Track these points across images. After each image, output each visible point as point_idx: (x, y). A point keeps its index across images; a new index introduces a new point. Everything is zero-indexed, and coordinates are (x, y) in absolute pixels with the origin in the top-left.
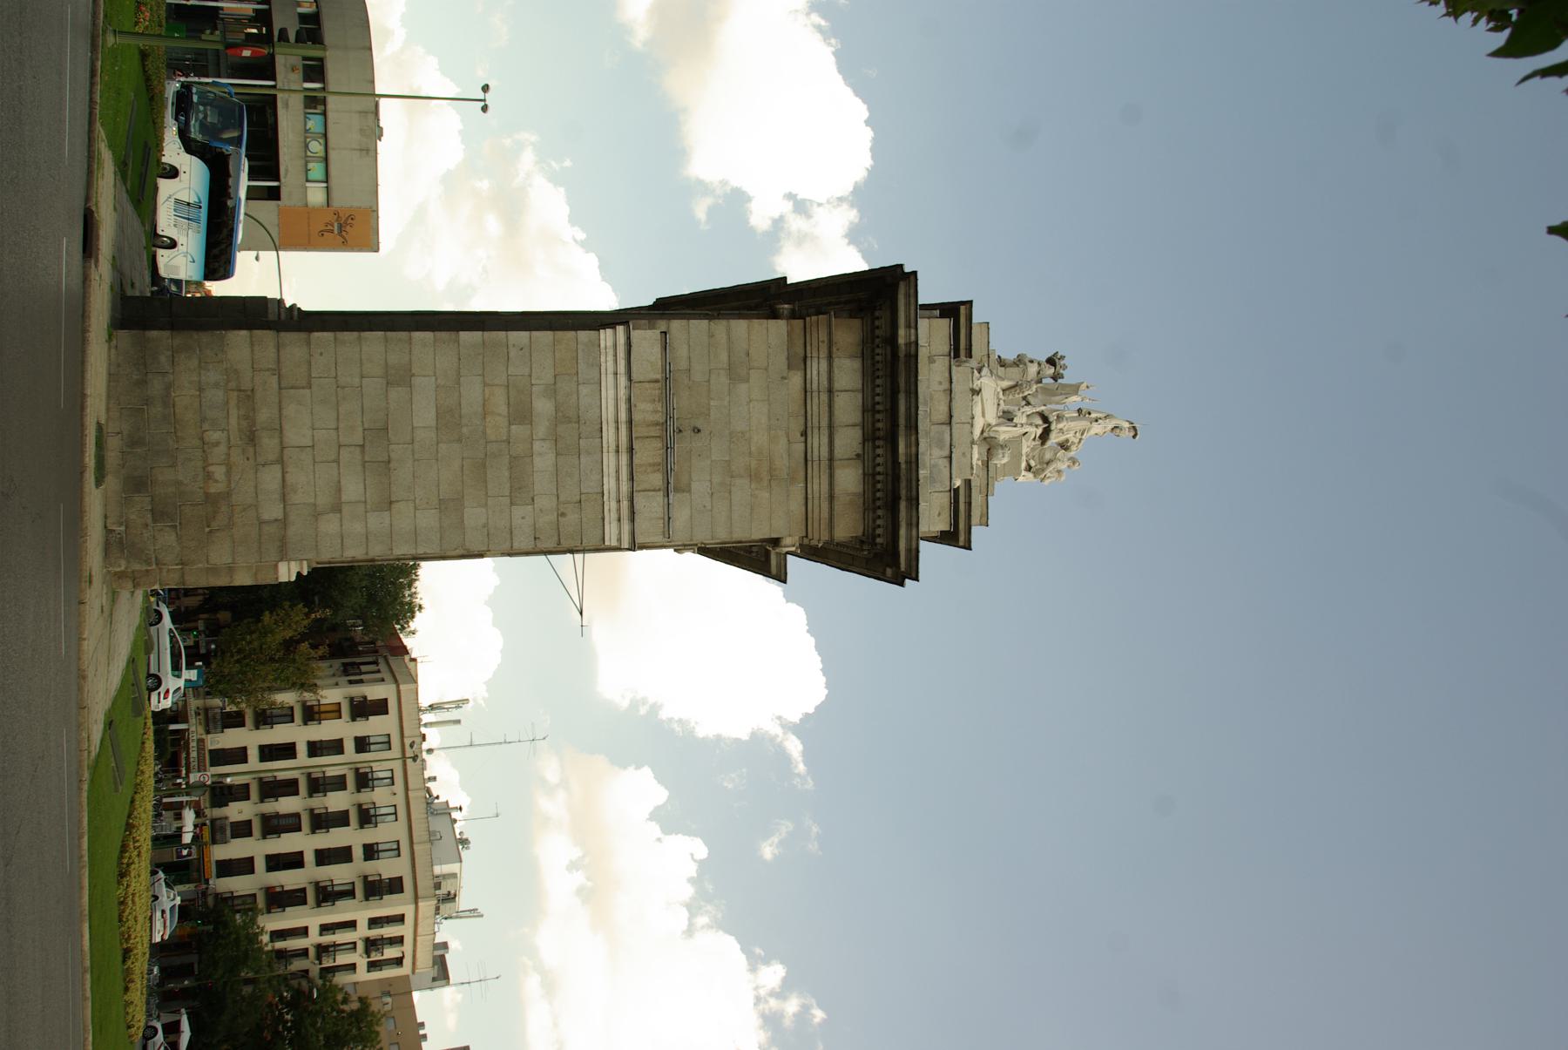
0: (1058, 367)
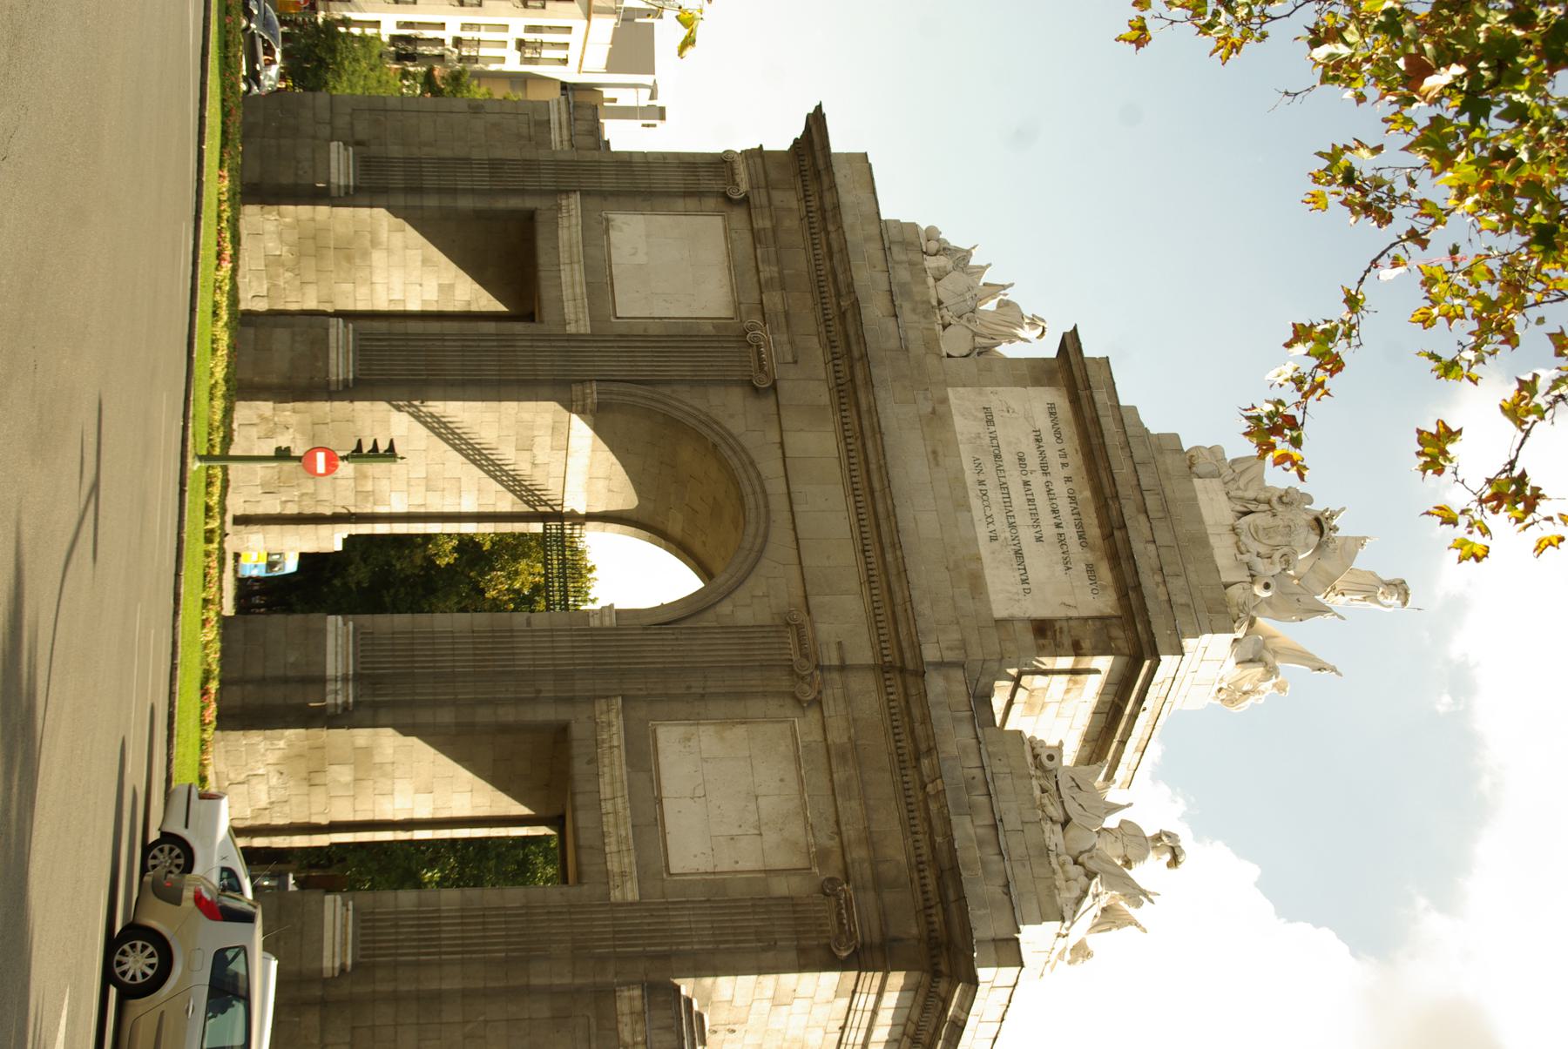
0: (1324, 539)
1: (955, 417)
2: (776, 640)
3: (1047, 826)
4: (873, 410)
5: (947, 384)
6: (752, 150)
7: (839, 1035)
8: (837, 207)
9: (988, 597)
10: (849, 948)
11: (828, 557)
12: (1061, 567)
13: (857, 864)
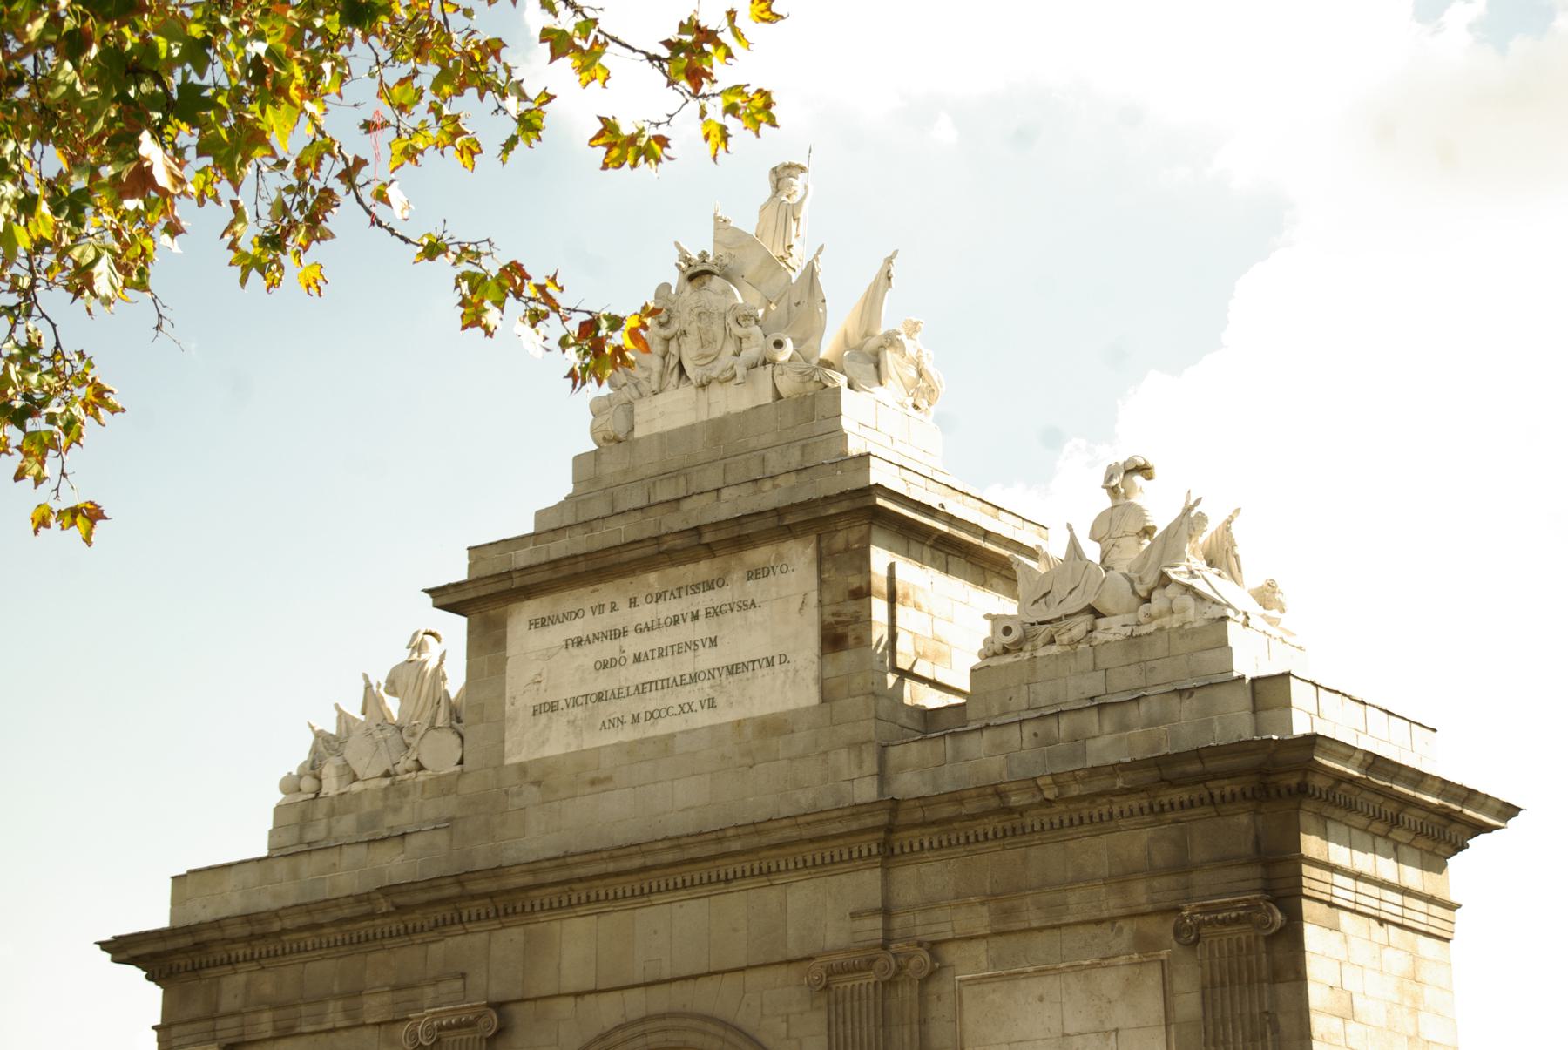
0: (716, 269)
1: (546, 755)
2: (848, 1005)
3: (1099, 636)
4: (533, 867)
5: (500, 766)
6: (159, 1040)
7: (1391, 928)
8: (247, 918)
9: (790, 712)
10: (1270, 910)
11: (735, 930)
12: (751, 613)
13: (1156, 897)
